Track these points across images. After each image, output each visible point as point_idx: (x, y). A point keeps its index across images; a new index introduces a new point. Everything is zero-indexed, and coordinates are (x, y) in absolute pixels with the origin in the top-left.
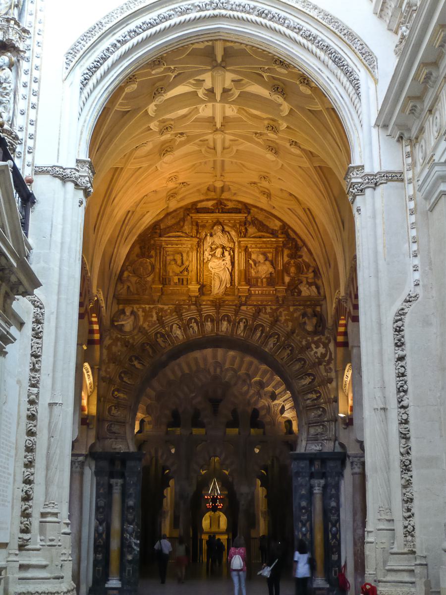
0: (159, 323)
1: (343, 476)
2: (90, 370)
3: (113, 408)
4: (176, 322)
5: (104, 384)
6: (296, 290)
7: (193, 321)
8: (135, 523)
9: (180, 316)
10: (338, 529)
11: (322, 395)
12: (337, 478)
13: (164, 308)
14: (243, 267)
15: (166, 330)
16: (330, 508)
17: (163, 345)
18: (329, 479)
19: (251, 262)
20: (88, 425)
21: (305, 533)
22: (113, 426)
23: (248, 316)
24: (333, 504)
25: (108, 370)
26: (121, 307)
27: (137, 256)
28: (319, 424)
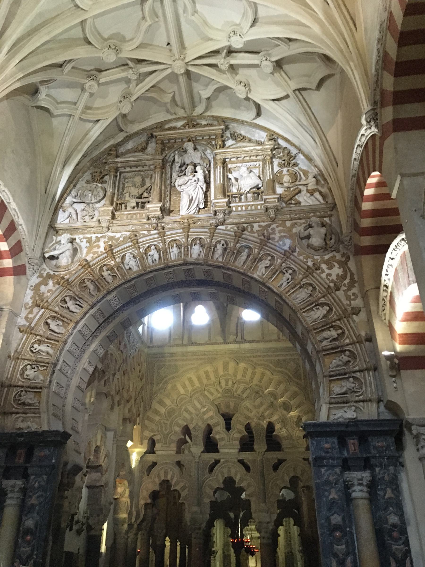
1: (402, 465)
3: (29, 367)
4: (130, 251)
6: (293, 202)
7: (153, 247)
11: (347, 332)
12: (391, 468)
13: (115, 236)
14: (219, 181)
16: (389, 527)
17: (110, 279)
18: (377, 469)
19: (230, 176)
22: (23, 393)
24: (393, 519)
25: (30, 316)
28: (347, 376)
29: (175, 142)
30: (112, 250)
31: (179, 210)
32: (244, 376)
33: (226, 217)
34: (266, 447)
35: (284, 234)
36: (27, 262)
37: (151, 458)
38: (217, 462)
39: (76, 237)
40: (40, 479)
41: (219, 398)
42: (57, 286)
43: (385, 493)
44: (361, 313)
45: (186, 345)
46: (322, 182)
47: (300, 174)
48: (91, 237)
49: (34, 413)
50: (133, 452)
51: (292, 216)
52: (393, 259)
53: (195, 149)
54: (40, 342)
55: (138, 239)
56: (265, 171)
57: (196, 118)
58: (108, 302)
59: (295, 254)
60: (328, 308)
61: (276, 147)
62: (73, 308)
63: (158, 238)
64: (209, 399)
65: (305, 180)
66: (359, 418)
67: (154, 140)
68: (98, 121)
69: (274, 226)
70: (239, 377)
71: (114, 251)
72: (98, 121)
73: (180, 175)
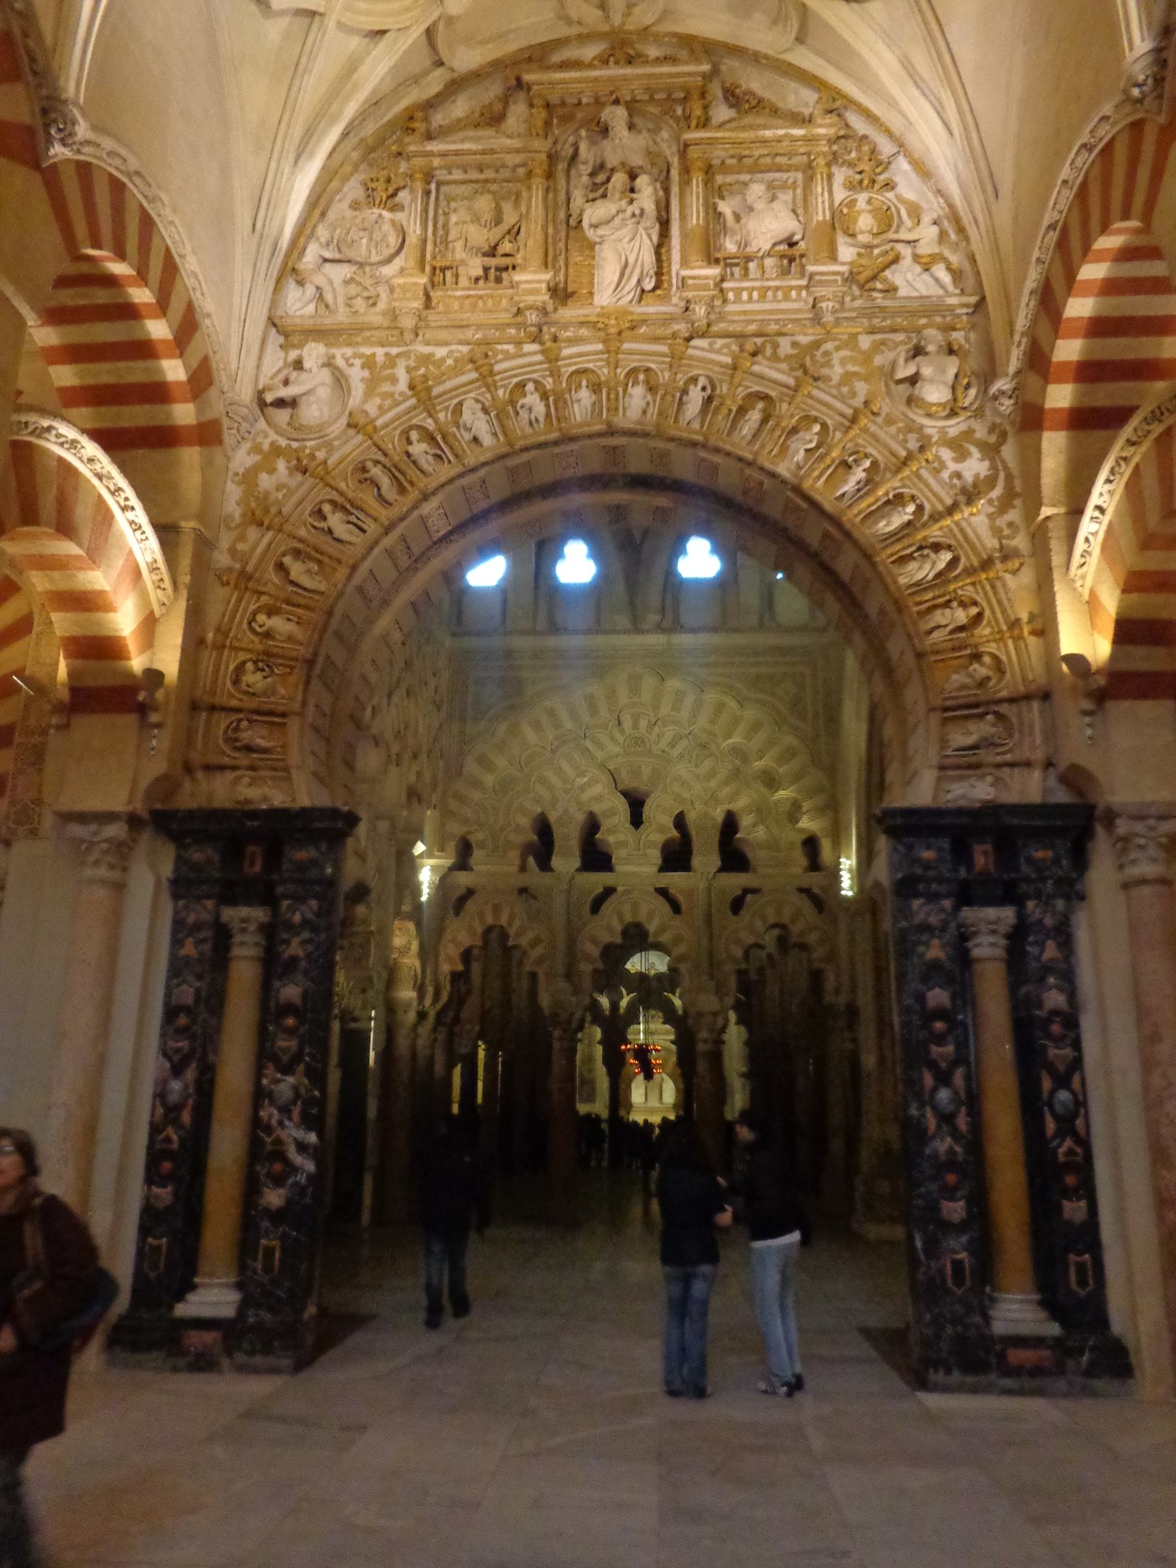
0: (415, 395)
1: (1082, 898)
2: (134, 501)
3: (250, 666)
5: (222, 592)
6: (879, 286)
7: (530, 387)
8: (301, 1067)
9: (487, 378)
10: (1081, 1098)
11: (987, 613)
12: (1060, 904)
14: (696, 217)
15: (436, 421)
17: (427, 462)
18: (1030, 904)
19: (725, 208)
20: (142, 709)
22: (245, 724)
23: (717, 369)
24: (1055, 999)
26: (293, 354)
27: (355, 206)
28: (980, 710)
30: (429, 389)
31: (591, 294)
32: (676, 707)
33: (713, 317)
34: (719, 863)
35: (856, 369)
36: (224, 413)
37: (463, 879)
38: (609, 891)
40: (303, 908)
41: (617, 755)
43: (1042, 951)
44: (1023, 569)
45: (541, 633)
46: (953, 236)
48: (374, 355)
49: (275, 769)
50: (422, 866)
51: (876, 321)
52: (1133, 444)
53: (631, 127)
54: (271, 612)
55: (492, 365)
56: (812, 199)
57: (635, 38)
58: (423, 520)
59: (880, 420)
60: (945, 557)
61: (842, 133)
63: (541, 363)
64: (593, 757)
67: (522, 95)
68: (382, 33)
69: (829, 346)
70: (665, 710)
71: (436, 391)
72: (382, 33)
73: (591, 196)
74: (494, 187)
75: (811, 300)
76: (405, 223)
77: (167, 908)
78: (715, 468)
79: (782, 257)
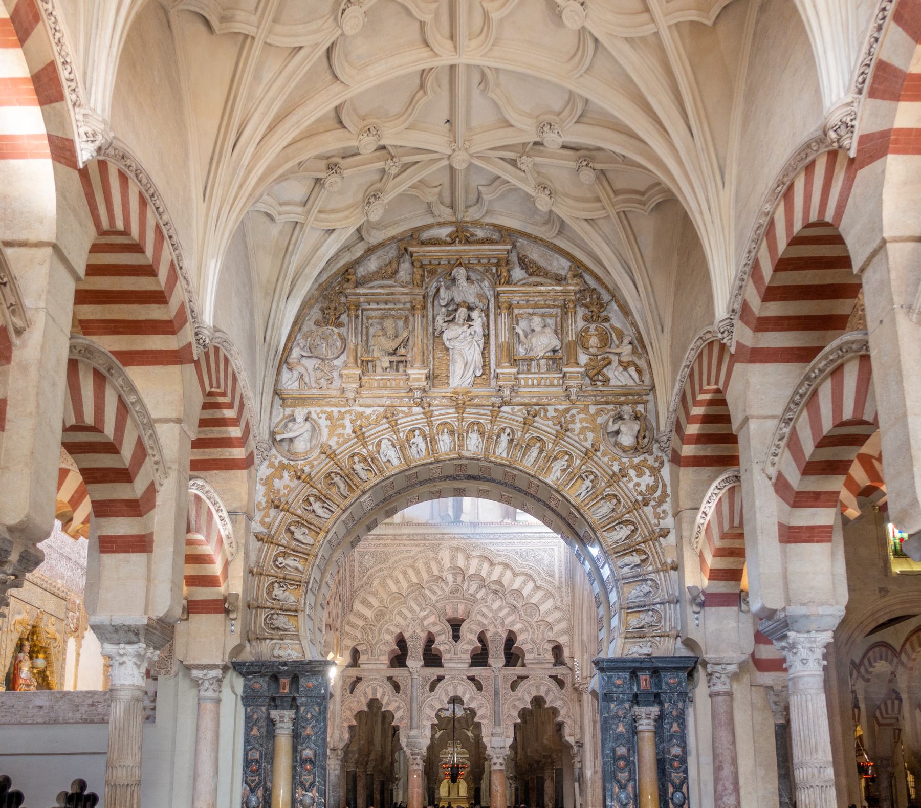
0: (357, 437)
3: (276, 585)
6: (600, 378)
9: (394, 425)
11: (651, 558)
12: (680, 705)
14: (504, 337)
17: (364, 475)
18: (666, 705)
19: (518, 330)
21: (625, 802)
22: (275, 616)
24: (676, 750)
25: (267, 520)
26: (288, 411)
29: (439, 264)
30: (364, 434)
31: (447, 376)
39: (312, 410)
40: (312, 710)
42: (296, 482)
43: (671, 727)
47: (611, 335)
53: (468, 279)
54: (284, 554)
59: (599, 454)
60: (633, 528)
62: (320, 511)
65: (617, 347)
66: (654, 655)
69: (574, 411)
71: (367, 435)
74: (393, 312)
75: (565, 388)
76: (345, 334)
77: (241, 709)
78: (515, 476)
79: (549, 358)
